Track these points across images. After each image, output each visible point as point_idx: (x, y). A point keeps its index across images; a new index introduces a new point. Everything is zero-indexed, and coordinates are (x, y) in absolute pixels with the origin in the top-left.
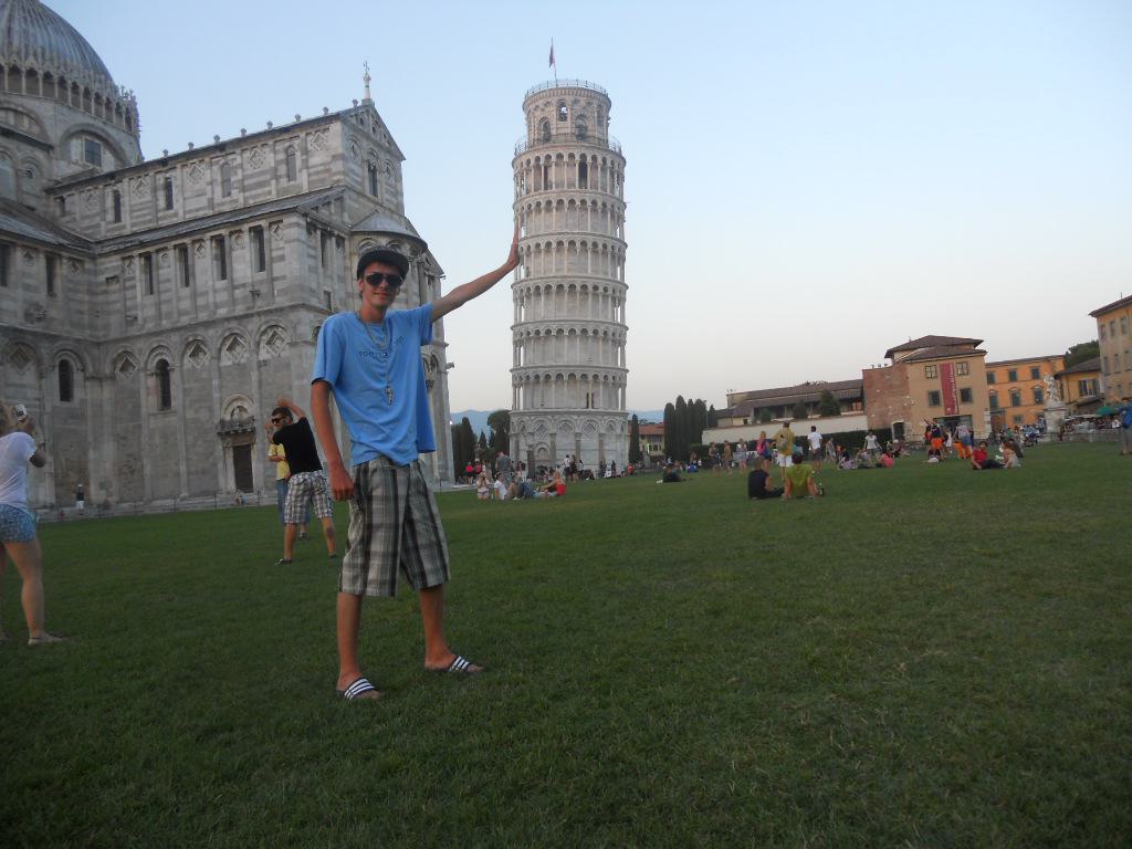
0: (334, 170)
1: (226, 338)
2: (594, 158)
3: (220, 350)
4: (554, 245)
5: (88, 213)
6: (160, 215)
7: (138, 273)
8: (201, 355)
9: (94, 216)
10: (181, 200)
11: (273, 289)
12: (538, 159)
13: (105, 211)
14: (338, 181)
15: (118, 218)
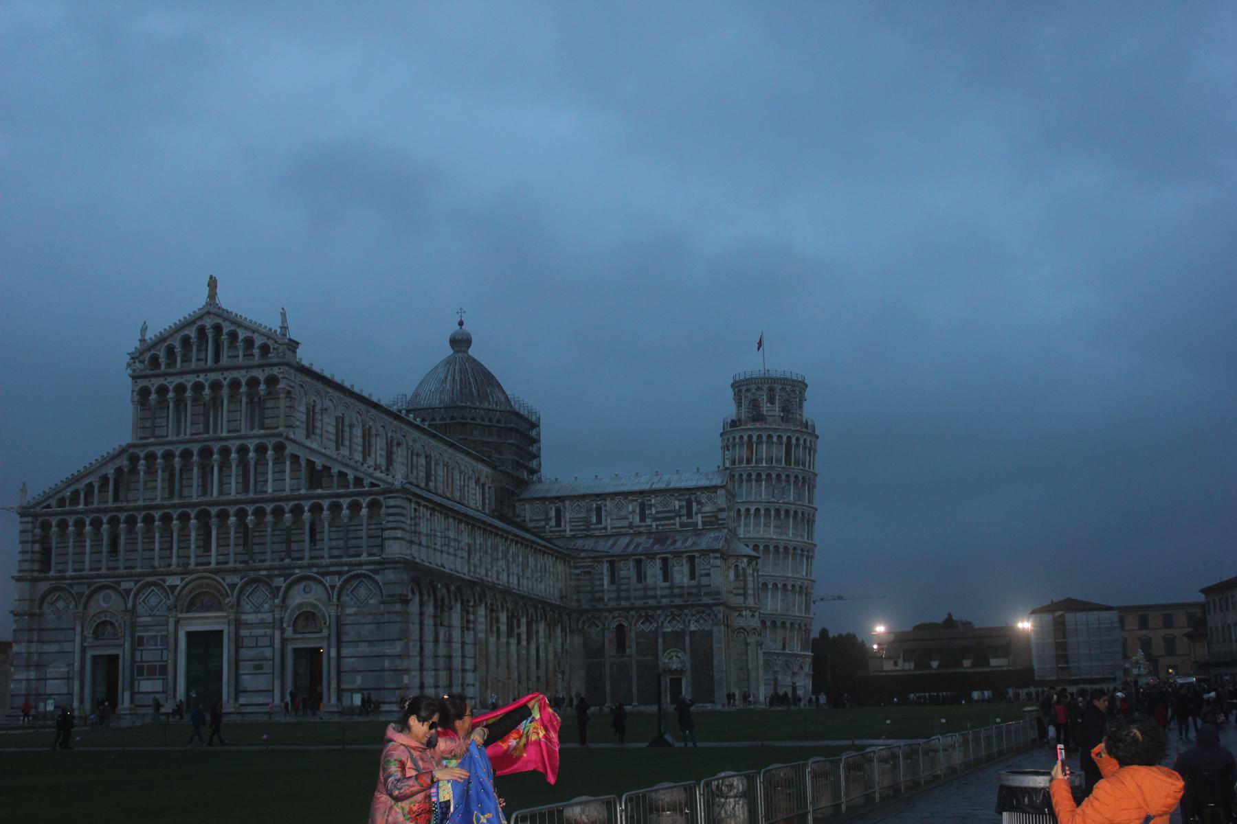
0: (720, 517)
1: (667, 616)
2: (798, 439)
3: (662, 622)
4: (762, 512)
5: (536, 518)
6: (592, 527)
7: (605, 572)
8: (647, 624)
9: (539, 521)
10: (609, 520)
11: (701, 592)
12: (750, 437)
13: (547, 520)
14: (723, 524)
15: (558, 524)
